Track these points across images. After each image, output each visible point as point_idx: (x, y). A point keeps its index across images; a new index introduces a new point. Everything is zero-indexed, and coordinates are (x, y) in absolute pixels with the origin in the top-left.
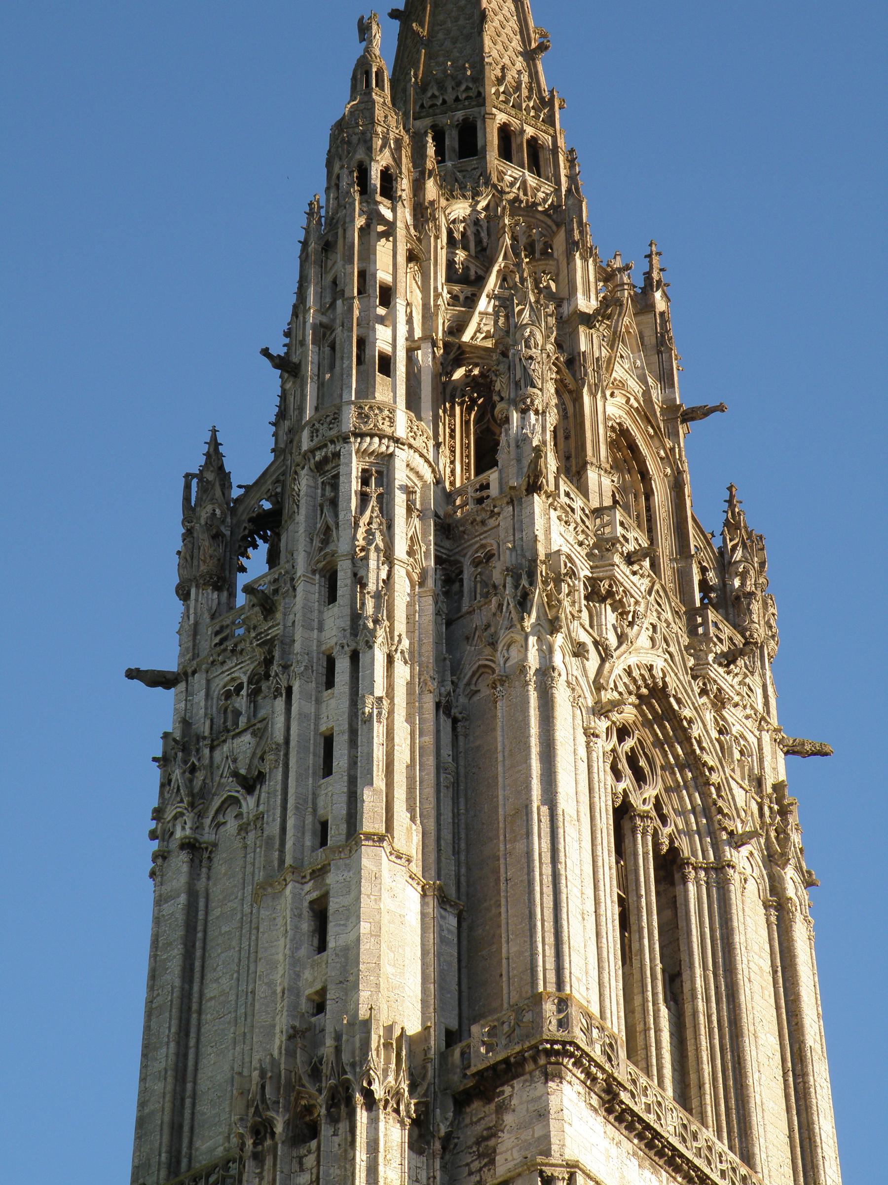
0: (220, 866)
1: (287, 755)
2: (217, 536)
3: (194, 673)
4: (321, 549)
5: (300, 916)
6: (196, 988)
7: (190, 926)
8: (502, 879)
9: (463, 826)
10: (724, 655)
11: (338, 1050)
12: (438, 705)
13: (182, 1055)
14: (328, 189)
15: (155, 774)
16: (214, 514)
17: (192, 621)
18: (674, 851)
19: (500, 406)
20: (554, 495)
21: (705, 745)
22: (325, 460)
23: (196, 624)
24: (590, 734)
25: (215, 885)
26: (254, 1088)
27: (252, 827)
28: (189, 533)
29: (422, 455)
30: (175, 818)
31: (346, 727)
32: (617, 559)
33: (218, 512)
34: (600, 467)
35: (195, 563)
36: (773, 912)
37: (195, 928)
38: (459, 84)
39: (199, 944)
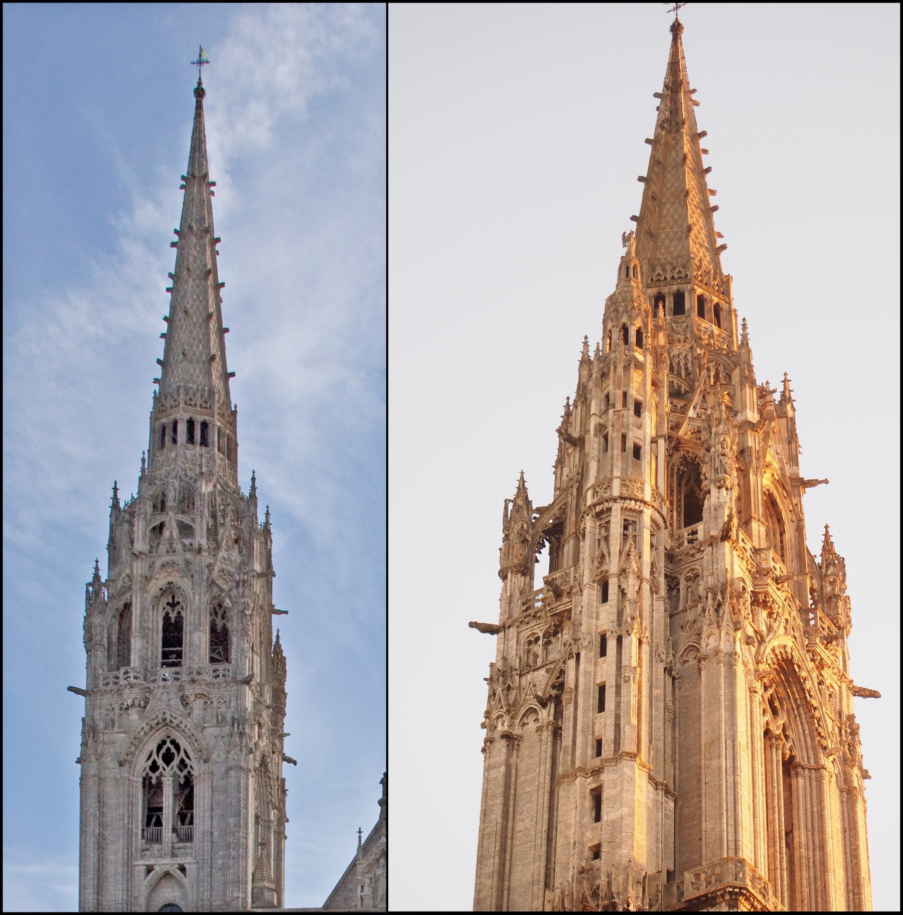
0: (525, 750)
1: (576, 696)
2: (524, 541)
3: (509, 627)
4: (598, 568)
5: (584, 798)
6: (510, 824)
7: (507, 786)
8: (703, 782)
9: (677, 745)
10: (825, 638)
11: (609, 884)
12: (665, 669)
13: (502, 864)
14: (603, 338)
15: (485, 689)
16: (522, 527)
17: (508, 594)
18: (792, 757)
19: (704, 483)
20: (737, 541)
21: (812, 693)
22: (602, 512)
23: (511, 596)
24: (753, 691)
25: (521, 761)
26: (557, 899)
27: (545, 729)
28: (506, 538)
29: (659, 512)
30: (498, 718)
31: (614, 683)
32: (769, 581)
33: (525, 526)
34: (759, 520)
35: (511, 557)
36: (845, 793)
37: (509, 787)
38: (674, 268)
39: (512, 797)
